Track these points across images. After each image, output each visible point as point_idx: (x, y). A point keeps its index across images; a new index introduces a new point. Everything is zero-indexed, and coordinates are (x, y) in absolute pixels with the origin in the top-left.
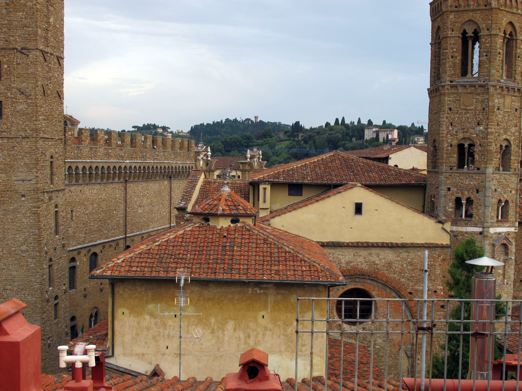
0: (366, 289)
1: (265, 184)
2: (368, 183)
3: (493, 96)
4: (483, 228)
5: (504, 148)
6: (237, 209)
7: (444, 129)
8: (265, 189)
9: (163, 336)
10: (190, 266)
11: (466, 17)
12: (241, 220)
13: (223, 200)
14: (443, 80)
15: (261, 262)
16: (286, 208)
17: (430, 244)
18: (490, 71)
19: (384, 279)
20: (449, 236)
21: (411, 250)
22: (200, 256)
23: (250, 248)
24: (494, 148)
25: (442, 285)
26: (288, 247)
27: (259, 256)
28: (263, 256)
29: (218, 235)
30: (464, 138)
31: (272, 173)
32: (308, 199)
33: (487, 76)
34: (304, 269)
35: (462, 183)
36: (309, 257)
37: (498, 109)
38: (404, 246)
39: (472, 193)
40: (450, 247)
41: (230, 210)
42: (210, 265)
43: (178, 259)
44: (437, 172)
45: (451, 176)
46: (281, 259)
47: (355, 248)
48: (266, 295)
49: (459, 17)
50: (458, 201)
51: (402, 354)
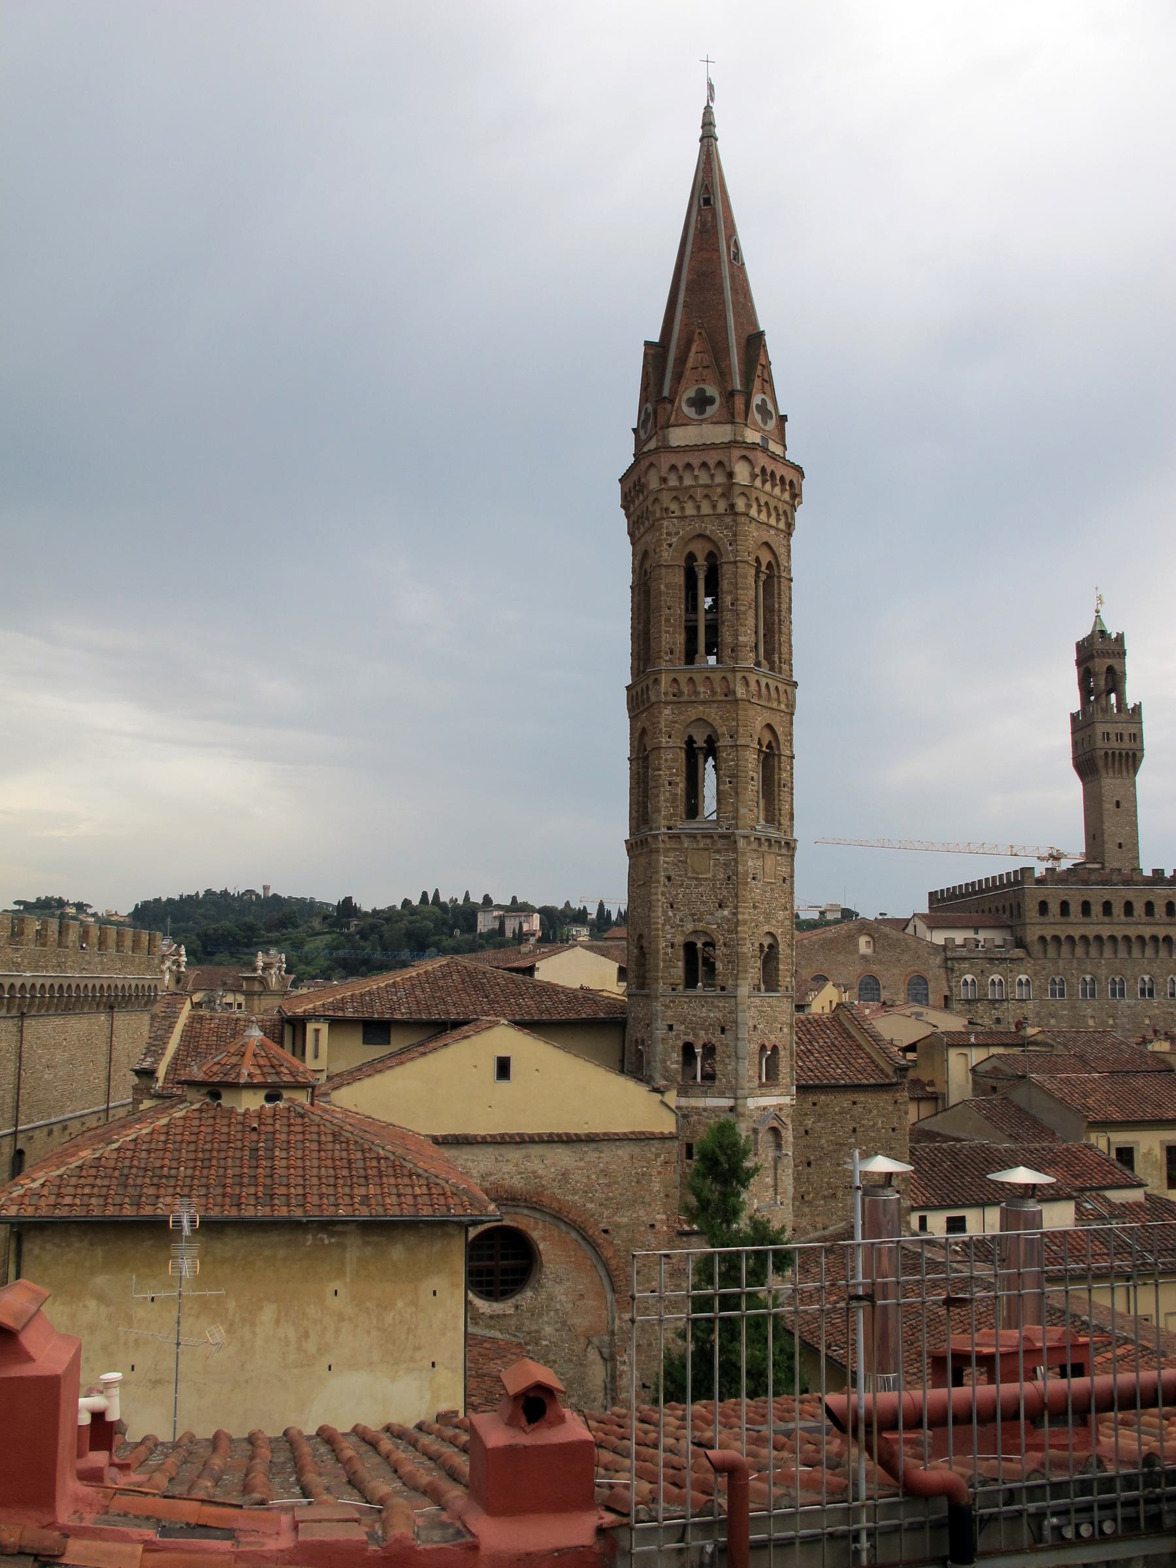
0: (522, 1227)
1: (317, 1021)
2: (518, 1018)
3: (744, 854)
4: (736, 1099)
5: (766, 949)
6: (278, 1073)
7: (659, 916)
8: (317, 1031)
9: (125, 1344)
10: (186, 1191)
11: (693, 713)
12: (286, 1094)
13: (249, 1054)
14: (654, 825)
15: (332, 1181)
16: (359, 1069)
17: (640, 1133)
18: (737, 810)
19: (555, 1205)
20: (673, 1117)
21: (605, 1147)
22: (205, 1171)
23: (307, 1152)
24: (749, 949)
25: (665, 1213)
26: (383, 1148)
27: (326, 1167)
28: (334, 1168)
29: (239, 1127)
30: (695, 932)
31: (330, 1000)
32: (402, 1052)
33: (733, 818)
34: (418, 1191)
35: (694, 1016)
36: (426, 1167)
37: (754, 878)
38: (591, 1139)
39: (713, 1034)
40: (677, 1138)
41: (263, 1074)
42: (228, 1190)
43: (161, 1177)
44: (647, 996)
45: (673, 1002)
46: (370, 1172)
47: (497, 1146)
48: (342, 1246)
49: (680, 713)
50: (688, 1051)
51: (593, 1355)
